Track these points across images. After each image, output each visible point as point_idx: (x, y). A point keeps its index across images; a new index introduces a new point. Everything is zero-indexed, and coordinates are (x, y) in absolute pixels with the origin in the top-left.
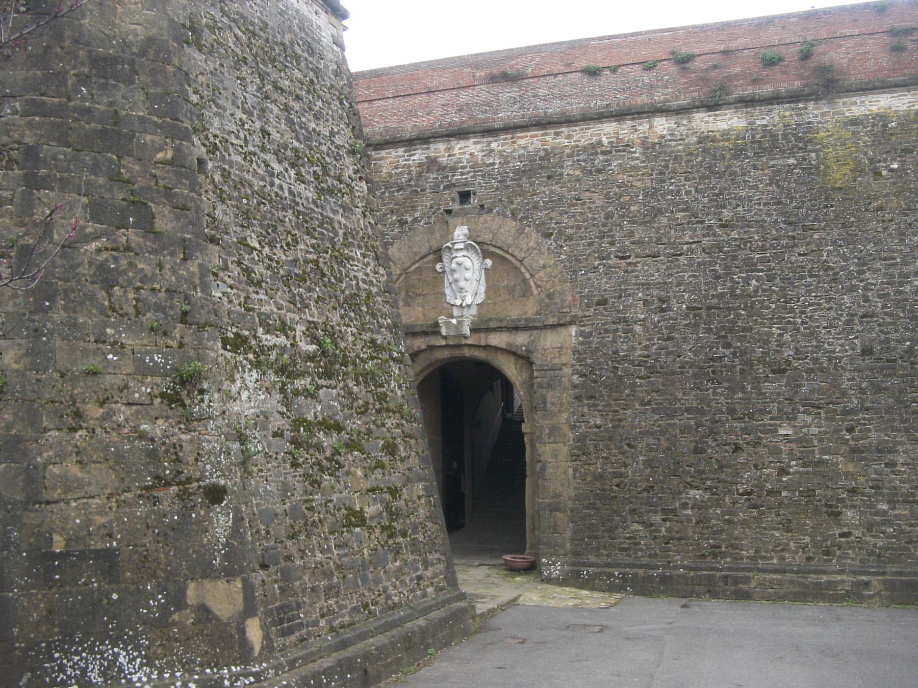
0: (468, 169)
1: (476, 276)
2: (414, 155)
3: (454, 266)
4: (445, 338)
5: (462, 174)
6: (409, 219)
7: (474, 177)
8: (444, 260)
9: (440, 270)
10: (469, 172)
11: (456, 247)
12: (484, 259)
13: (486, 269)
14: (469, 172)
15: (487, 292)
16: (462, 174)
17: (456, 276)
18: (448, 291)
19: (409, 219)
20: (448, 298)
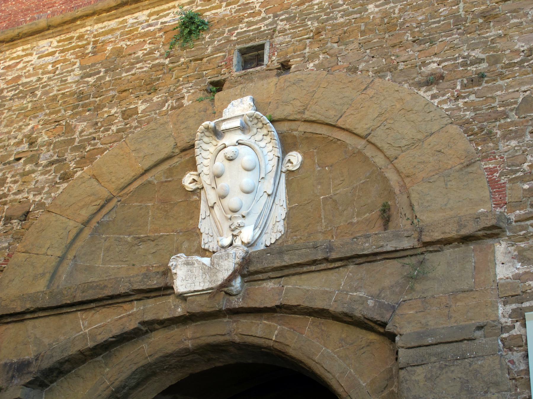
0: (263, 15)
1: (268, 186)
2: (168, 15)
3: (220, 163)
4: (183, 297)
5: (249, 24)
6: (141, 107)
7: (274, 22)
8: (199, 159)
9: (191, 187)
10: (264, 19)
11: (224, 126)
12: (285, 152)
13: (289, 173)
14: (264, 19)
15: (288, 217)
16: (249, 24)
17: (222, 183)
18: (204, 226)
19: (141, 107)
20: (205, 238)
